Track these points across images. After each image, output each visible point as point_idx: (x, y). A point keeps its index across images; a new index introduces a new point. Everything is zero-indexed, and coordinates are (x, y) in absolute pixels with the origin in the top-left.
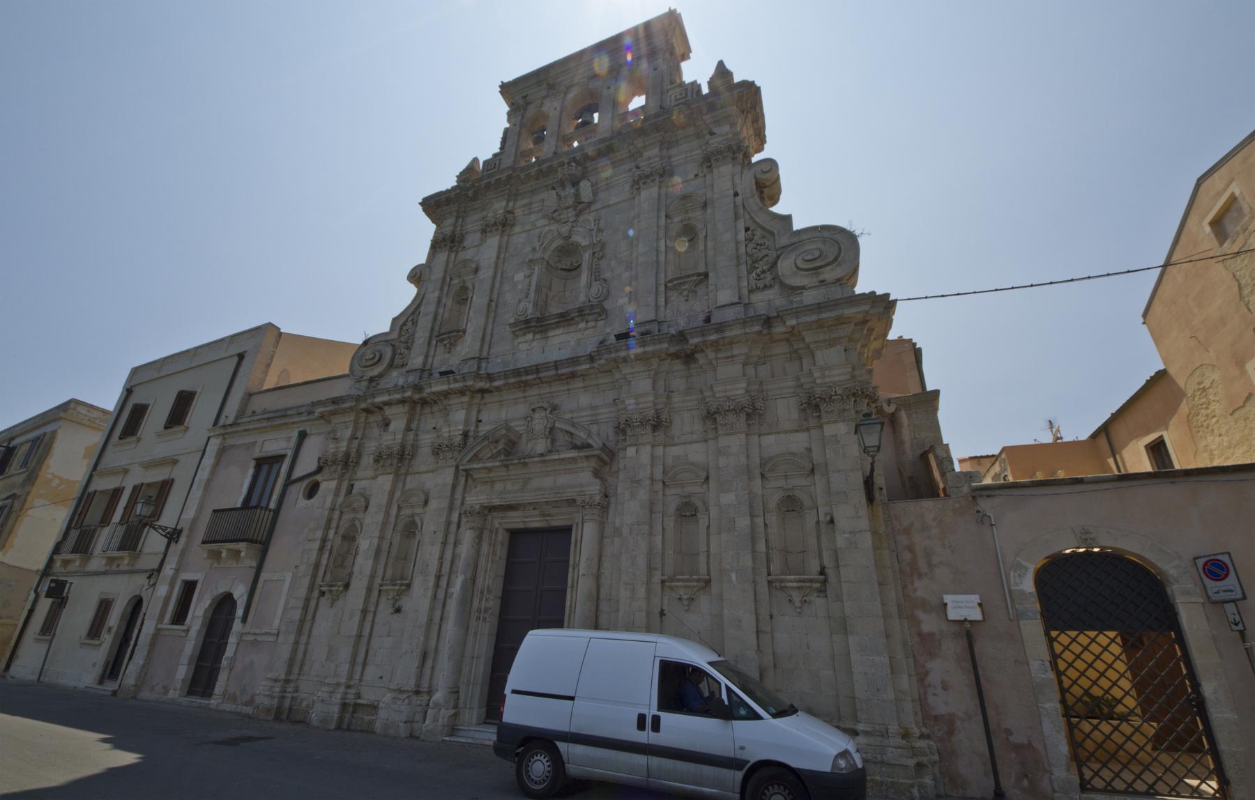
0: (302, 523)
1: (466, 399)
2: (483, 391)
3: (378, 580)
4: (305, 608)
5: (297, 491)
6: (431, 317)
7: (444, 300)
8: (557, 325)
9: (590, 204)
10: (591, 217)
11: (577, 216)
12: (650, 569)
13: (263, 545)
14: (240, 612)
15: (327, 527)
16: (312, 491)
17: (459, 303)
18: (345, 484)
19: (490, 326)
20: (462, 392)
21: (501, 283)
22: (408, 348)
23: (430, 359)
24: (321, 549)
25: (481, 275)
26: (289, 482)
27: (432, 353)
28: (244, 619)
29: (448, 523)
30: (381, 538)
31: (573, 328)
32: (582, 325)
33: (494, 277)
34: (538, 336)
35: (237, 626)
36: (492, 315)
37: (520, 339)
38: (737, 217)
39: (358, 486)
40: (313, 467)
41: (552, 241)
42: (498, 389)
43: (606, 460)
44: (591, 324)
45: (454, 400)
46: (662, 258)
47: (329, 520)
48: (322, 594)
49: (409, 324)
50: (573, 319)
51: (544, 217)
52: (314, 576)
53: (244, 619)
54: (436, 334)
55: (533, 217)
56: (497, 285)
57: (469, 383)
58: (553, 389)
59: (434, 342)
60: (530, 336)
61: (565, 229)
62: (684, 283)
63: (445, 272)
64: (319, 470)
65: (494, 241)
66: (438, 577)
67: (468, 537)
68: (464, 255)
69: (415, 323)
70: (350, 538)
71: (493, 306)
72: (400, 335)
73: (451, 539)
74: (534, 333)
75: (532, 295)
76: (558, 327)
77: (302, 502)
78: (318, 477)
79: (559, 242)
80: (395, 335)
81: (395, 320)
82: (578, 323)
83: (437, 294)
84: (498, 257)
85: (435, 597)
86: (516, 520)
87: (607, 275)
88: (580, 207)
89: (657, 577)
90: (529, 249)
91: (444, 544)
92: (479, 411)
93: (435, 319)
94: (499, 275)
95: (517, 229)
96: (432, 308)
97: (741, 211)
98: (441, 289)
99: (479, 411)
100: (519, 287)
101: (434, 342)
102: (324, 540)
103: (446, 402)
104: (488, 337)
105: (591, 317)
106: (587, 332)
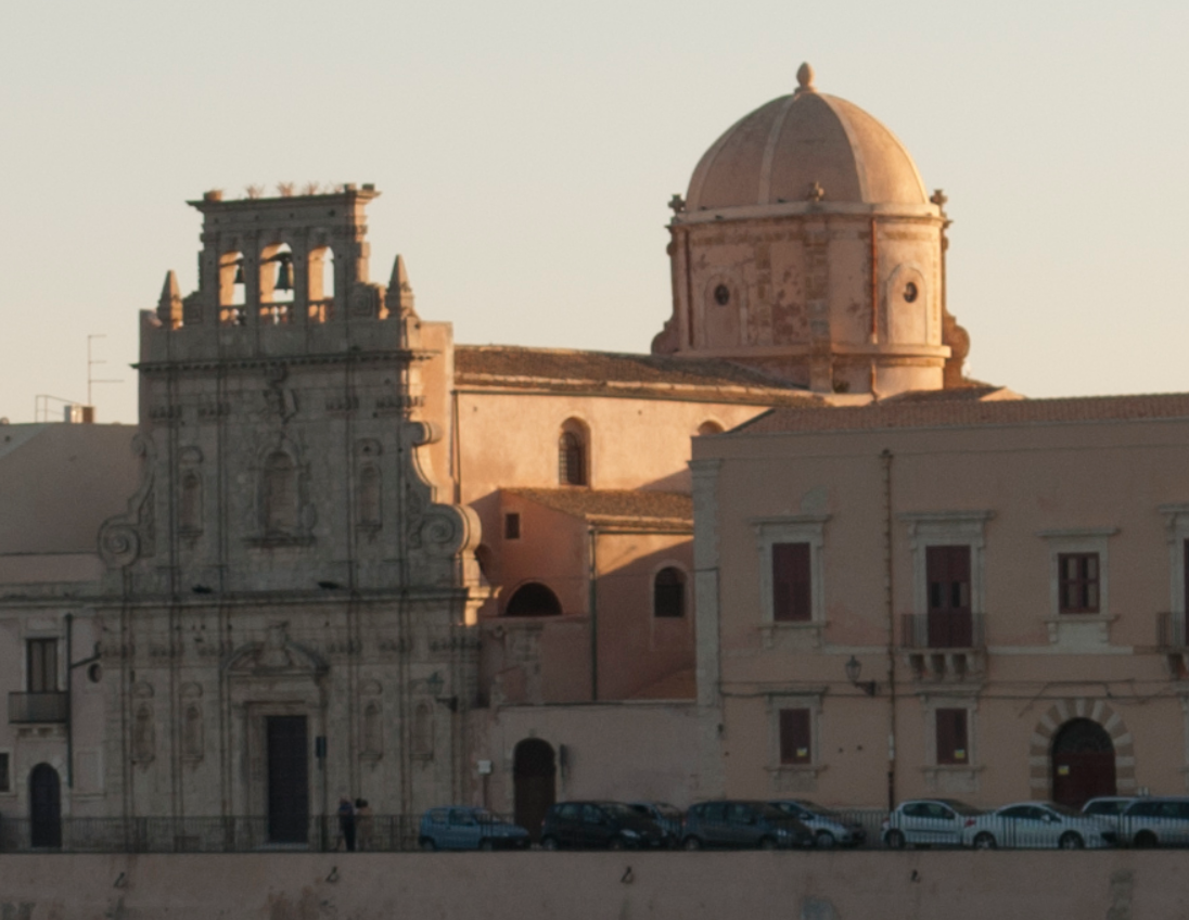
0: (94, 706)
3: (177, 754)
4: (124, 775)
5: (81, 674)
9: (293, 415)
12: (351, 748)
13: (65, 720)
14: (64, 779)
15: (123, 710)
16: (94, 674)
18: (127, 672)
24: (123, 728)
26: (71, 667)
28: (71, 784)
29: (222, 712)
30: (173, 721)
33: (219, 477)
35: (64, 790)
39: (139, 674)
40: (89, 653)
43: (322, 671)
47: (123, 704)
48: (134, 763)
52: (124, 750)
53: (71, 784)
64: (97, 656)
66: (222, 751)
67: (237, 724)
70: (143, 716)
73: (226, 724)
77: (90, 685)
78: (98, 662)
79: (271, 450)
80: (134, 519)
84: (219, 451)
85: (222, 765)
86: (269, 710)
89: (356, 752)
91: (222, 728)
93: (171, 509)
101: (175, 536)
102: (124, 721)
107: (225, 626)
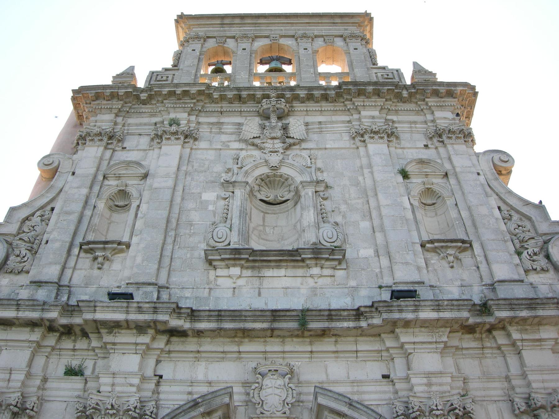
1: (145, 339)
2: (175, 333)
6: (74, 218)
7: (92, 201)
8: (278, 264)
10: (305, 154)
11: (287, 149)
17: (110, 208)
19: (169, 247)
20: (141, 328)
21: (183, 199)
22: (34, 252)
23: (68, 272)
25: (155, 182)
27: (71, 263)
31: (300, 272)
32: (316, 271)
34: (248, 273)
36: (172, 233)
37: (220, 272)
38: (487, 195)
41: (256, 167)
42: (199, 333)
44: (327, 272)
45: (125, 337)
46: (410, 215)
49: (36, 219)
50: (303, 260)
51: (240, 141)
54: (79, 240)
55: (224, 138)
56: (178, 199)
57: (161, 317)
58: (288, 348)
59: (76, 251)
60: (235, 271)
61: (274, 159)
62: (447, 247)
63: (98, 169)
65: (172, 151)
68: (121, 156)
69: (45, 220)
71: (172, 226)
72: (20, 231)
74: (242, 267)
75: (236, 221)
76: (278, 267)
79: (264, 170)
81: (13, 210)
82: (308, 267)
83: (85, 191)
87: (339, 219)
88: (289, 142)
90: (218, 168)
92: (158, 362)
93: (80, 221)
94: (180, 188)
95: (202, 144)
96: (77, 207)
97: (488, 189)
98: (91, 188)
99: (158, 362)
100: (211, 208)
101: (76, 251)
103: (108, 338)
104: (166, 261)
105: (328, 263)
106: (321, 281)
107: (149, 372)
